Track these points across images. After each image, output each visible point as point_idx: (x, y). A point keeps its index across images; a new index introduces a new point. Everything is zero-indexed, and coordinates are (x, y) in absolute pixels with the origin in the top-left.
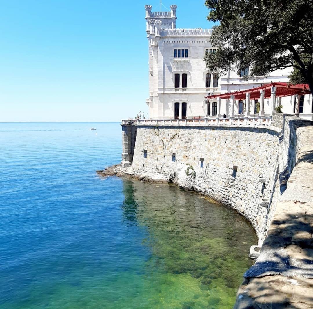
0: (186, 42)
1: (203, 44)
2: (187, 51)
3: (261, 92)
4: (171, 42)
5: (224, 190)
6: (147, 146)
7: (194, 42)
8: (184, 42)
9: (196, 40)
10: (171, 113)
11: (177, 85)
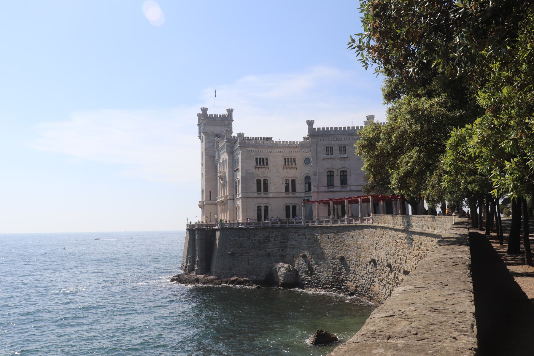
0: (266, 151)
1: (281, 154)
2: (267, 159)
3: (359, 199)
4: (253, 151)
5: (331, 278)
6: (234, 249)
7: (273, 151)
8: (264, 151)
9: (275, 150)
10: (254, 215)
11: (259, 190)
